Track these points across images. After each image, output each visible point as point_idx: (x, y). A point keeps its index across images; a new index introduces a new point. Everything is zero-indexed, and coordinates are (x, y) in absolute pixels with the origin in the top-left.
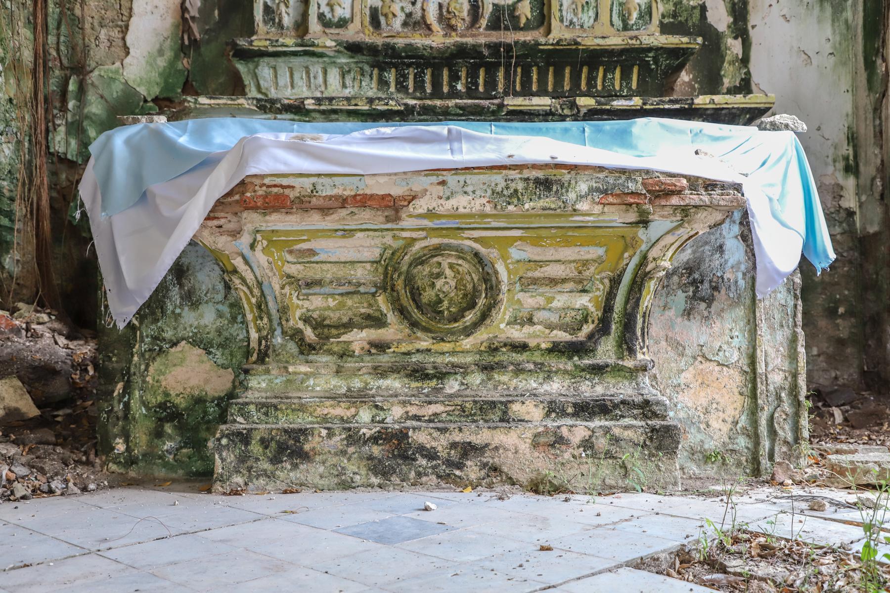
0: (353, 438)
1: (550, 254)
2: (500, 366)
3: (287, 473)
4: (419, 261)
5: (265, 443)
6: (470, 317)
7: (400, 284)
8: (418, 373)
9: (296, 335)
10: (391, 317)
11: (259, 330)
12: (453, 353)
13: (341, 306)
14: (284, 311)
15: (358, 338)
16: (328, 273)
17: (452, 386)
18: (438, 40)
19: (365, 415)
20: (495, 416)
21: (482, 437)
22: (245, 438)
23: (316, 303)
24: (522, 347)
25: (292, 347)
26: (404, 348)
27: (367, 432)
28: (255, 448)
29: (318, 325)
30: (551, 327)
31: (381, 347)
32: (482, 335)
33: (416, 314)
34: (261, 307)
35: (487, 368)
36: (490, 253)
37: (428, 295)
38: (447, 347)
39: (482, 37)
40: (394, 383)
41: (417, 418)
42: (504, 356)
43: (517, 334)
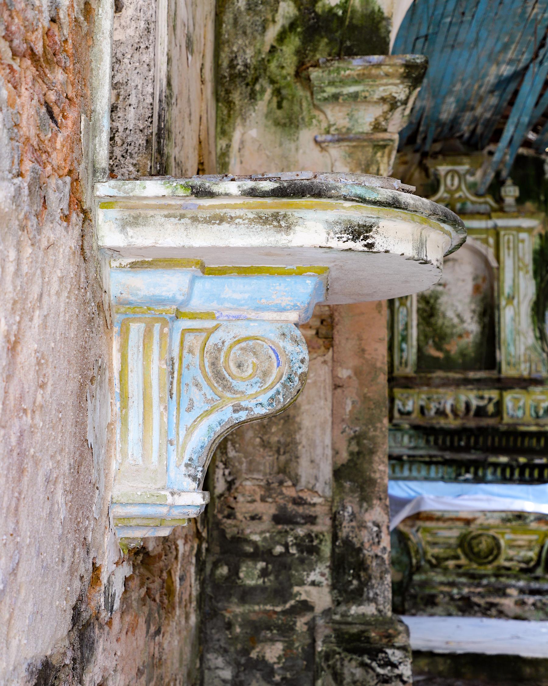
0: (452, 598)
1: (519, 537)
2: (502, 576)
3: (430, 610)
4: (474, 538)
5: (422, 599)
6: (491, 558)
7: (466, 545)
8: (472, 576)
9: (429, 562)
10: (462, 556)
11: (416, 559)
12: (485, 570)
13: (444, 552)
14: (425, 553)
15: (451, 563)
16: (441, 540)
17: (485, 582)
18: (452, 423)
19: (455, 591)
20: (501, 593)
21: (496, 600)
22: (414, 597)
23: (436, 551)
24: (508, 569)
25: (427, 566)
26: (467, 567)
27: (457, 597)
28: (419, 600)
29: (437, 558)
30: (519, 562)
31: (459, 567)
32: (495, 564)
33: (471, 556)
34: (417, 552)
35: (497, 576)
36: (499, 536)
37: (476, 550)
38: (482, 568)
39: (472, 423)
40: (463, 580)
41: (473, 593)
42: (503, 572)
43: (507, 564)
